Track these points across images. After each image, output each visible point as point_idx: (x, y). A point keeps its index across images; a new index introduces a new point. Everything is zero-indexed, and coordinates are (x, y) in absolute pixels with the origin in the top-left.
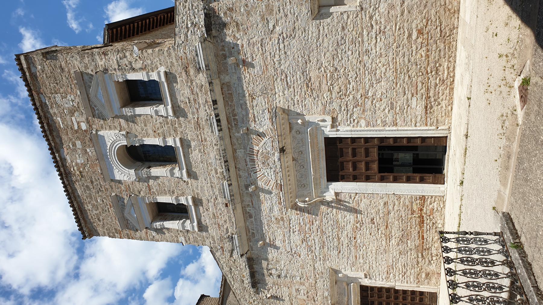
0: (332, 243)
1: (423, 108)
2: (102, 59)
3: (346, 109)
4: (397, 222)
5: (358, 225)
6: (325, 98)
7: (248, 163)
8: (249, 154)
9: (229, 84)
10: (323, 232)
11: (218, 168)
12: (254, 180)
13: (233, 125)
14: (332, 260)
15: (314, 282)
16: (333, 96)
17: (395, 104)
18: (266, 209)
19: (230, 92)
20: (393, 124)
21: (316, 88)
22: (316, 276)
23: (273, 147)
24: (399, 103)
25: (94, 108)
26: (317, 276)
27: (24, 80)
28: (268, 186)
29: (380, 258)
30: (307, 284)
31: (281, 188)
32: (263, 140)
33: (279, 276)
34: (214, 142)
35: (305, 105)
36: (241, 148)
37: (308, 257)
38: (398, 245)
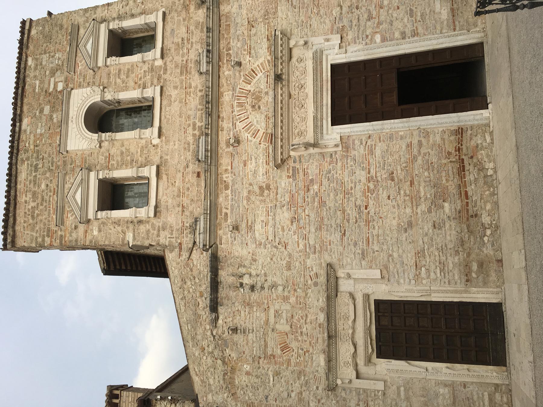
0: (334, 219)
1: (449, 10)
2: (104, 10)
3: (358, 24)
4: (426, 174)
5: (371, 186)
6: (334, 14)
7: (235, 108)
8: (238, 96)
9: (229, 15)
10: (322, 203)
11: (197, 121)
12: (239, 131)
13: (225, 61)
14: (333, 251)
15: (303, 295)
16: (343, 12)
17: (415, 10)
18: (248, 173)
19: (228, 23)
20: (413, 34)
21: (325, 4)
22: (307, 282)
23: (267, 83)
24: (419, 8)
25: (78, 64)
26: (310, 282)
27: (19, 43)
28: (256, 138)
29: (404, 239)
30: (293, 300)
31: (272, 139)
32: (256, 75)
33: (252, 288)
34: (200, 87)
35: (311, 26)
36: (229, 90)
37: (298, 247)
38: (430, 211)
